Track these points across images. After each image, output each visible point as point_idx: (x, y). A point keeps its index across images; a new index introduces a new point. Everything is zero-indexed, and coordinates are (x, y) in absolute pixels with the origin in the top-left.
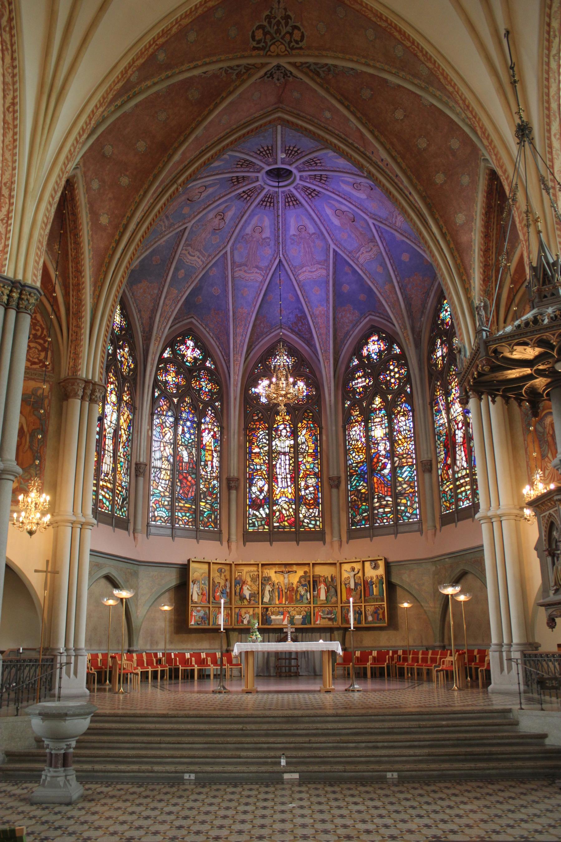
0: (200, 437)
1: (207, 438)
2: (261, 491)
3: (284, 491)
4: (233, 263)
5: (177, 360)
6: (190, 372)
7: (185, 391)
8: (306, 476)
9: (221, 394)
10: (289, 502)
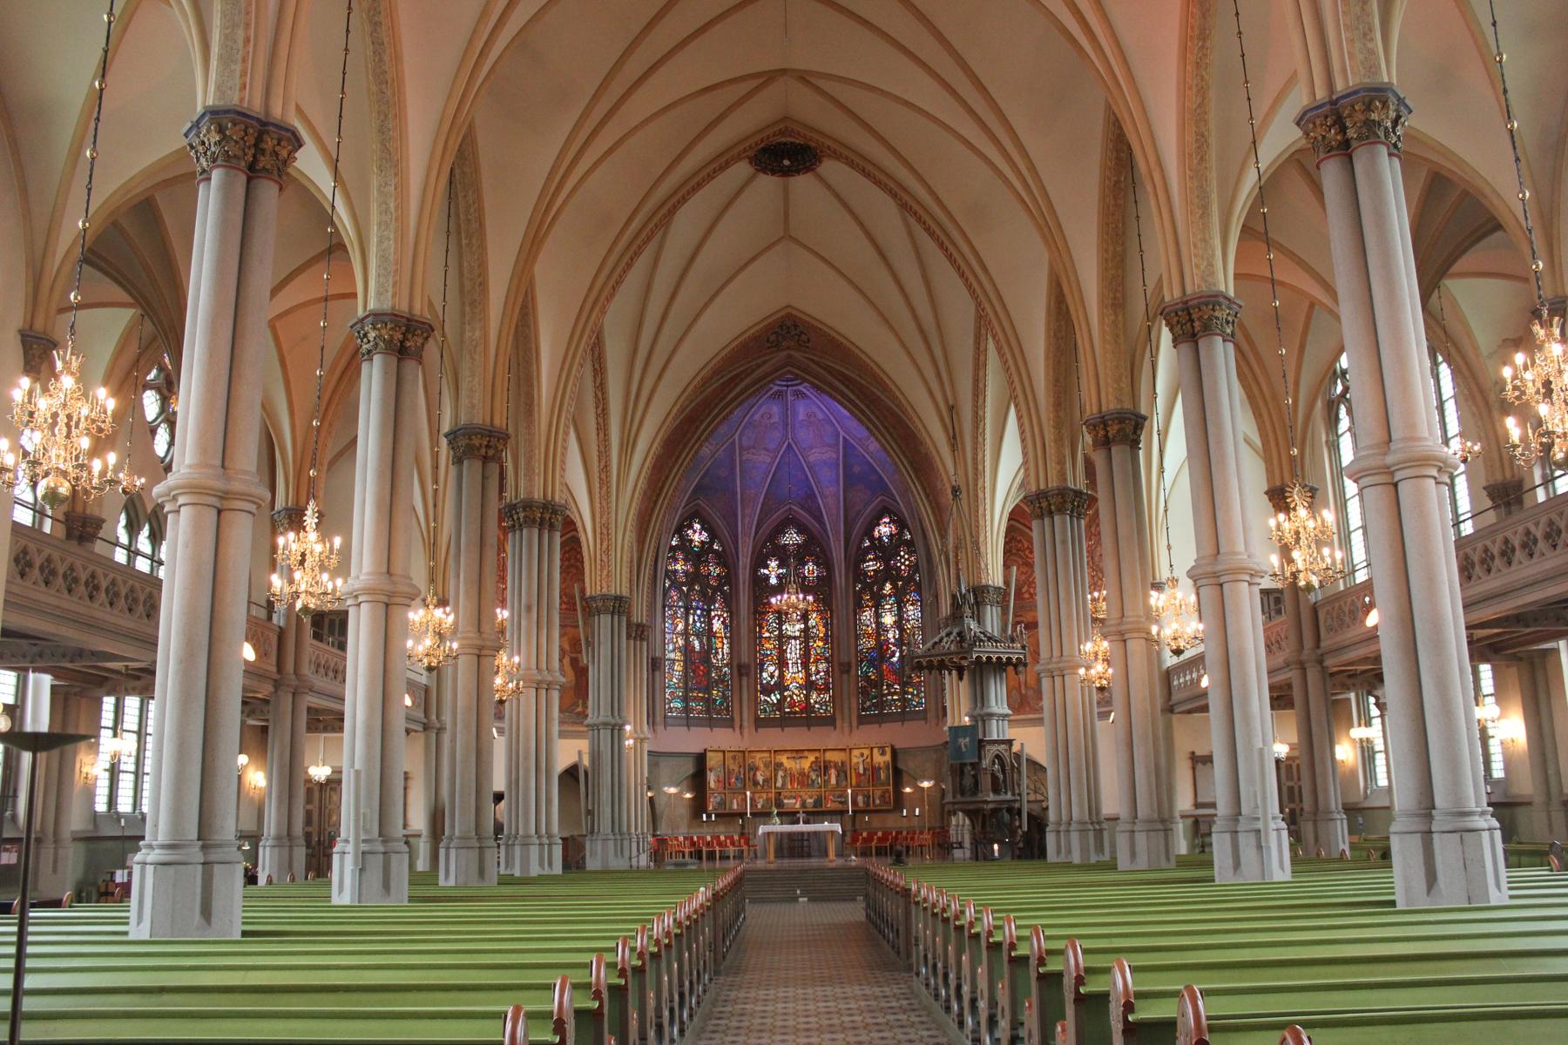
0: (710, 625)
1: (717, 625)
2: (772, 676)
3: (795, 675)
4: (741, 447)
5: (685, 544)
6: (697, 557)
7: (694, 578)
8: (816, 661)
9: (729, 578)
10: (800, 687)
